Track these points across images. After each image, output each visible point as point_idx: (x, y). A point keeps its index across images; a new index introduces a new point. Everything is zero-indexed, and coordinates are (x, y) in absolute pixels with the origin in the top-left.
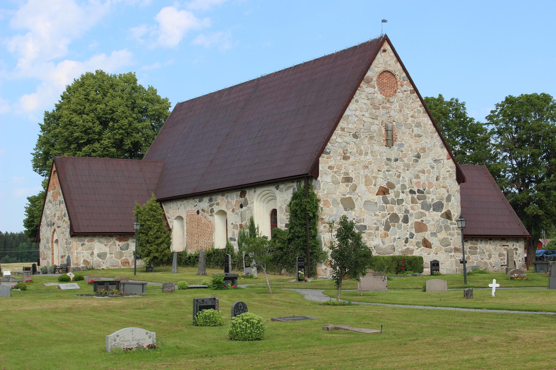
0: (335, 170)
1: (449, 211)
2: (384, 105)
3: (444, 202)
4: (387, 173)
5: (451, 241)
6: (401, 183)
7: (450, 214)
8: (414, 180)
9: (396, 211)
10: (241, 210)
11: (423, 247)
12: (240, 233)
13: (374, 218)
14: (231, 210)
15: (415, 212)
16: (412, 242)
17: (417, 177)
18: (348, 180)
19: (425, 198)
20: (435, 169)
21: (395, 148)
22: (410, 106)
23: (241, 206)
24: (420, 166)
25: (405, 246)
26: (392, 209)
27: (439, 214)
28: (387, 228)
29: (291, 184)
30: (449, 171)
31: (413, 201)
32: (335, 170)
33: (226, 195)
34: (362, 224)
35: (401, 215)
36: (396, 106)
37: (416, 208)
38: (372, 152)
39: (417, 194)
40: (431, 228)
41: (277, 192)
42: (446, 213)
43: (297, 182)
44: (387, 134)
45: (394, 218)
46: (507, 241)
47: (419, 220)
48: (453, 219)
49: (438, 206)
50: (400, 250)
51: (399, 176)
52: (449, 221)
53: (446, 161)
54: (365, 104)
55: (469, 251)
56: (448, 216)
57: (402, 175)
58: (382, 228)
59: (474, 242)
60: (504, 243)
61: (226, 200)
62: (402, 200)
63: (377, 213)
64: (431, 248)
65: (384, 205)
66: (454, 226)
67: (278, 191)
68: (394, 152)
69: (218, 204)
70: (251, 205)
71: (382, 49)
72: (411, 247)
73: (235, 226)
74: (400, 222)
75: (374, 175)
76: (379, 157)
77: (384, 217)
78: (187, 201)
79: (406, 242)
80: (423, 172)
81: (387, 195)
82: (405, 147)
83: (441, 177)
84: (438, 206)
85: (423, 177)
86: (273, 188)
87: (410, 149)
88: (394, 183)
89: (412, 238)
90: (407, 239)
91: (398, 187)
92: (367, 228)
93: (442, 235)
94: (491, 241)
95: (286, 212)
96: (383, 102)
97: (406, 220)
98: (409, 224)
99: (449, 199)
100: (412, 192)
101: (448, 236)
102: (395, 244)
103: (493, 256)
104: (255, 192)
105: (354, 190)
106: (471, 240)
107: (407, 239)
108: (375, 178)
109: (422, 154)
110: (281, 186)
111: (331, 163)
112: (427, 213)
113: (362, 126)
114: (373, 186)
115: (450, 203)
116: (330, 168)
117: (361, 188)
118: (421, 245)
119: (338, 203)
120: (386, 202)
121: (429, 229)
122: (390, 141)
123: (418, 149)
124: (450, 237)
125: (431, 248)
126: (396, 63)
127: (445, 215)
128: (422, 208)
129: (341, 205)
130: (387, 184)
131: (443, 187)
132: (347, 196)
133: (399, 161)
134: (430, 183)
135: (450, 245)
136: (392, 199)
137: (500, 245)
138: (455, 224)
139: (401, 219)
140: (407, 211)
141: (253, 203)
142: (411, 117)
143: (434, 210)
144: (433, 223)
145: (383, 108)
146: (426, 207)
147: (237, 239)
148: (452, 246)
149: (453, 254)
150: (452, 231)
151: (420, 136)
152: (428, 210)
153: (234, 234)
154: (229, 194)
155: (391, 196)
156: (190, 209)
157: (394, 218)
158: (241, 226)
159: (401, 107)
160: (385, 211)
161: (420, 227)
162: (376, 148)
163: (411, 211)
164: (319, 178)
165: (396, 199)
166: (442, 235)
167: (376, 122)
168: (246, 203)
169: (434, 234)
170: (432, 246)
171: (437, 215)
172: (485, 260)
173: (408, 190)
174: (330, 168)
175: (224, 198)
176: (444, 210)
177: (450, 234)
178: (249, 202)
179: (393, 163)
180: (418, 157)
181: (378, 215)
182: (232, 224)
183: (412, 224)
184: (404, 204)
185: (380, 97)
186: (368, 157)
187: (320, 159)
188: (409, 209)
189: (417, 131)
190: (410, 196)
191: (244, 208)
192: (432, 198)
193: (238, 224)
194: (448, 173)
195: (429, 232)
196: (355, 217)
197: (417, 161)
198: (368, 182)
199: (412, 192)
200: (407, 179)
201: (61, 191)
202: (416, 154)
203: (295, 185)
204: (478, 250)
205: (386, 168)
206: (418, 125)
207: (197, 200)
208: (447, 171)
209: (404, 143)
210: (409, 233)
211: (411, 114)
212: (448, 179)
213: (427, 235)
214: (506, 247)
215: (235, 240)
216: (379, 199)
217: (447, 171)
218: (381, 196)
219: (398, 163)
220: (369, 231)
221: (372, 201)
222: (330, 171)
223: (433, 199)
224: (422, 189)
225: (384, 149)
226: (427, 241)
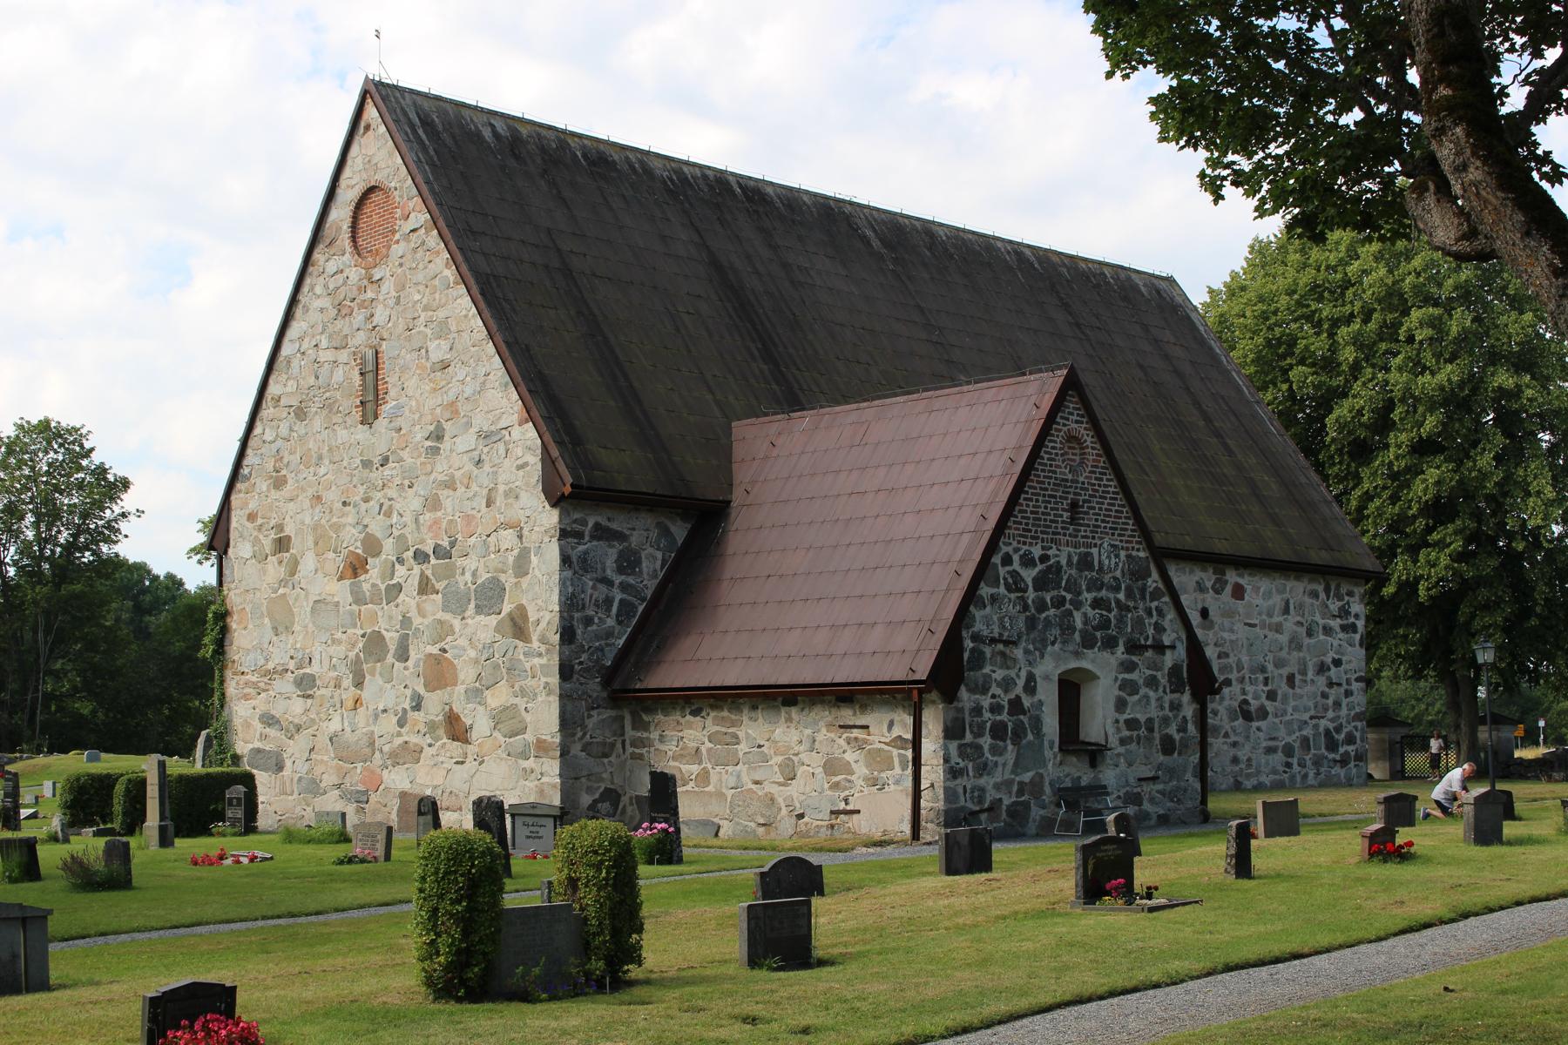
0: (260, 521)
1: (521, 609)
2: (362, 297)
3: (508, 579)
4: (364, 506)
5: (528, 718)
6: (396, 533)
7: (525, 617)
8: (428, 517)
9: (382, 625)
11: (445, 740)
13: (333, 650)
15: (426, 622)
16: (416, 722)
17: (433, 503)
18: (282, 544)
19: (449, 573)
20: (487, 468)
21: (381, 423)
22: (420, 277)
24: (441, 468)
25: (399, 734)
26: (374, 618)
27: (493, 620)
28: (359, 684)
30: (526, 464)
31: (425, 587)
32: (260, 521)
34: (308, 671)
35: (392, 637)
36: (388, 287)
37: (428, 607)
38: (330, 450)
39: (433, 561)
40: (466, 674)
42: (511, 617)
44: (364, 385)
45: (375, 643)
46: (864, 708)
47: (434, 650)
48: (535, 638)
49: (489, 596)
50: (386, 748)
51: (388, 514)
52: (520, 644)
53: (516, 432)
54: (322, 310)
55: (709, 750)
56: (518, 627)
57: (397, 506)
58: (347, 682)
59: (725, 713)
60: (847, 715)
62: (399, 588)
63: (339, 635)
64: (467, 741)
65: (354, 607)
66: (536, 661)
68: (379, 438)
71: (363, 124)
72: (414, 739)
74: (390, 659)
75: (335, 520)
76: (345, 463)
77: (354, 645)
79: (401, 723)
80: (450, 485)
81: (362, 578)
82: (406, 409)
83: (501, 488)
84: (489, 596)
85: (449, 500)
87: (417, 416)
88: (379, 535)
89: (417, 707)
90: (405, 710)
91: (388, 546)
92: (318, 682)
93: (499, 697)
94: (794, 711)
96: (359, 289)
97: (403, 656)
98: (410, 663)
99: (521, 567)
100: (421, 557)
101: (517, 701)
102: (377, 730)
103: (801, 771)
105: (293, 574)
106: (713, 707)
107: (405, 710)
108: (337, 528)
109: (447, 426)
111: (252, 505)
112: (457, 623)
113: (312, 381)
114: (331, 555)
115: (525, 581)
116: (251, 517)
117: (308, 563)
118: (441, 732)
119: (262, 616)
120: (359, 599)
121: (461, 676)
122: (370, 405)
123: (438, 410)
124: (521, 703)
125: (467, 741)
126: (390, 155)
127: (508, 623)
128: (445, 608)
129: (266, 620)
130: (364, 542)
131: (507, 526)
132: (281, 591)
133: (391, 465)
134: (469, 519)
135: (524, 730)
136: (374, 585)
137: (830, 726)
138: (540, 655)
139: (392, 647)
140: (406, 621)
142: (426, 309)
143: (479, 610)
144: (472, 654)
145: (361, 306)
146: (455, 603)
148: (529, 737)
149: (530, 763)
150: (530, 682)
151: (445, 366)
152: (461, 612)
155: (373, 575)
157: (375, 643)
159: (401, 287)
160: (355, 626)
161: (439, 672)
162: (342, 434)
163: (417, 621)
164: (230, 551)
165: (383, 587)
166: (499, 697)
167: (343, 356)
169: (475, 694)
170: (474, 735)
171: (484, 627)
172: (769, 788)
173: (410, 553)
174: (251, 517)
176: (507, 608)
177: (523, 693)
179: (376, 476)
180: (438, 435)
181: (340, 642)
183: (416, 665)
184: (402, 596)
185: (354, 274)
186: (322, 471)
187: (233, 498)
188: (413, 614)
189: (438, 350)
190: (417, 570)
192: (472, 568)
194: (521, 473)
195: (460, 689)
196: (292, 652)
197: (435, 451)
198: (321, 541)
199: (421, 557)
200: (408, 518)
202: (432, 428)
204: (743, 748)
205: (361, 489)
206: (442, 330)
208: (520, 467)
209: (403, 400)
210: (408, 692)
211: (425, 301)
212: (523, 495)
213: (457, 698)
214: (856, 733)
216: (341, 591)
217: (520, 467)
218: (347, 582)
219: (387, 471)
220: (323, 691)
221: (329, 599)
222: (249, 525)
223: (474, 574)
224: (445, 543)
225: (361, 433)
226: (458, 718)
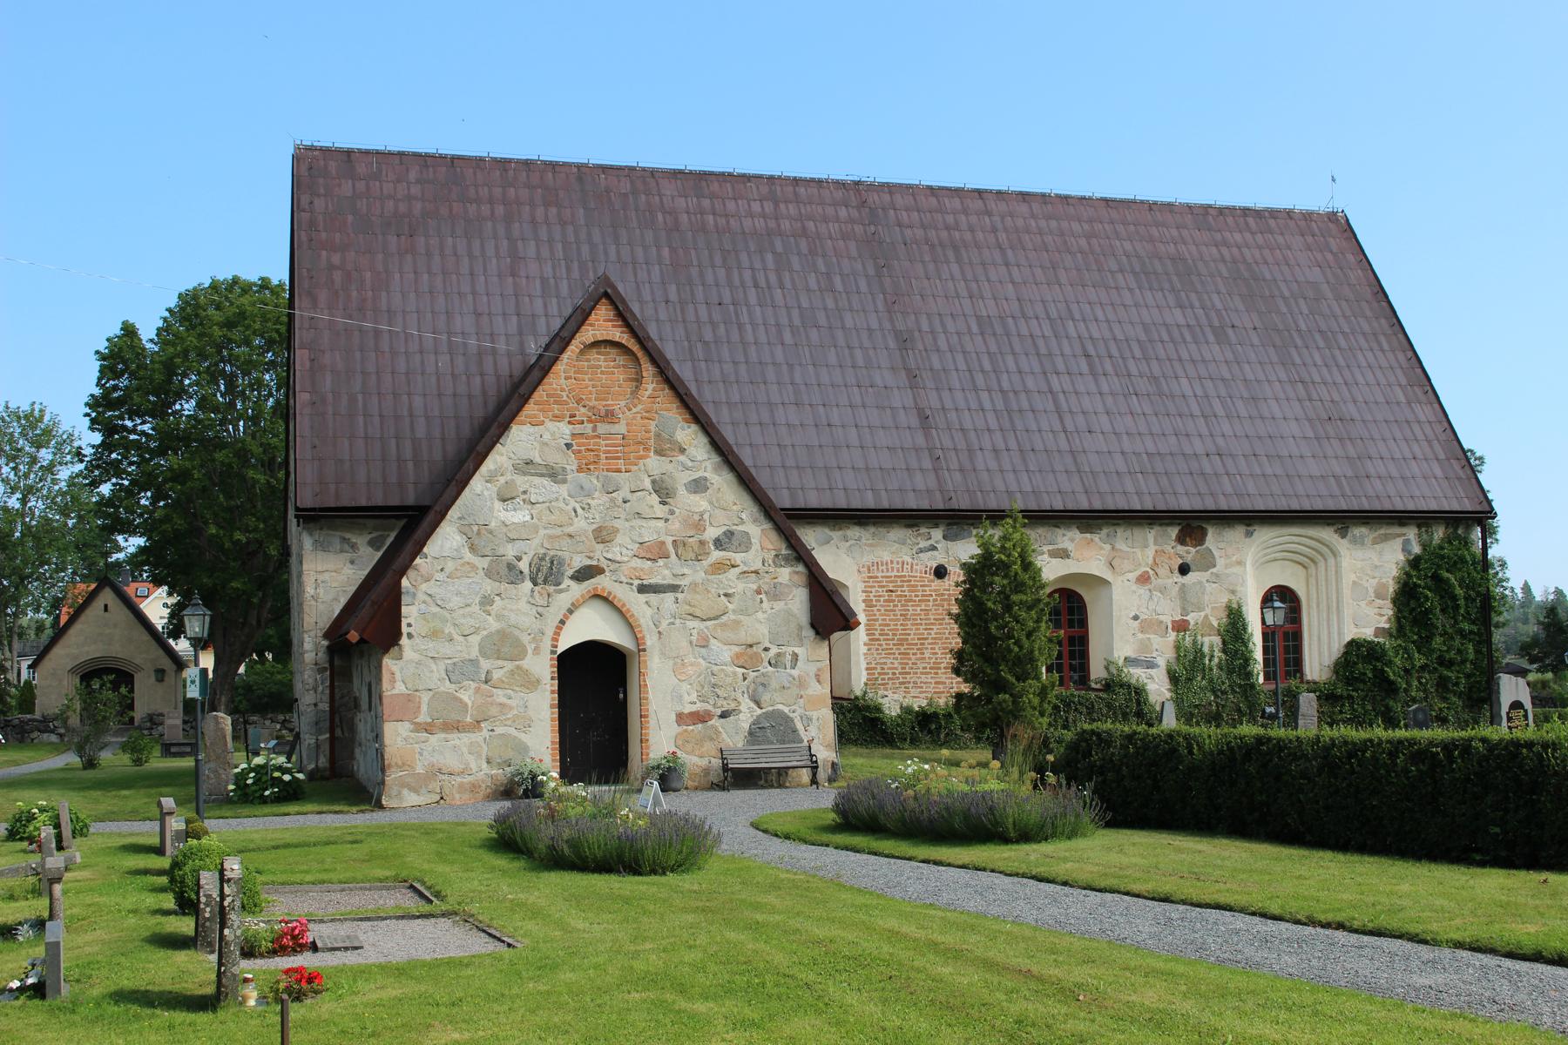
10: (1177, 577)
12: (1178, 647)
14: (1133, 576)
23: (1184, 570)
29: (1397, 530)
33: (1105, 531)
41: (1341, 545)
43: (1419, 526)
61: (1108, 547)
67: (1344, 542)
69: (1063, 554)
70: (1236, 569)
73: (1147, 626)
78: (872, 529)
86: (1327, 534)
95: (1379, 596)
104: (1249, 534)
110: (1358, 531)
141: (1240, 563)
147: (1162, 662)
153: (1145, 646)
154: (1120, 531)
156: (886, 557)
158: (1180, 627)
168: (1208, 563)
175: (1096, 537)
178: (1220, 562)
182: (1136, 618)
191: (1192, 577)
193: (1167, 620)
201: (688, 435)
203: (1411, 533)
207: (937, 534)
215: (1151, 665)
